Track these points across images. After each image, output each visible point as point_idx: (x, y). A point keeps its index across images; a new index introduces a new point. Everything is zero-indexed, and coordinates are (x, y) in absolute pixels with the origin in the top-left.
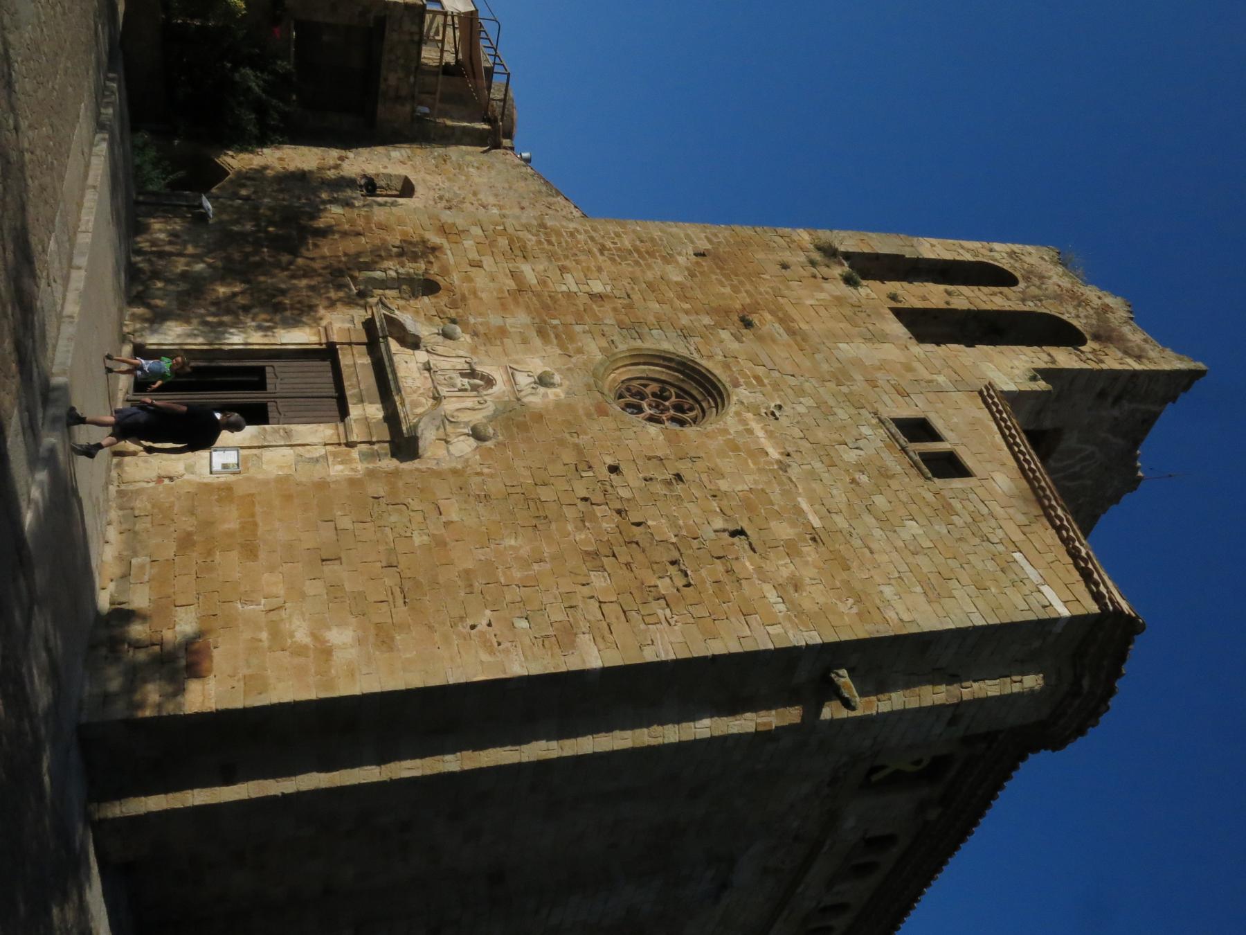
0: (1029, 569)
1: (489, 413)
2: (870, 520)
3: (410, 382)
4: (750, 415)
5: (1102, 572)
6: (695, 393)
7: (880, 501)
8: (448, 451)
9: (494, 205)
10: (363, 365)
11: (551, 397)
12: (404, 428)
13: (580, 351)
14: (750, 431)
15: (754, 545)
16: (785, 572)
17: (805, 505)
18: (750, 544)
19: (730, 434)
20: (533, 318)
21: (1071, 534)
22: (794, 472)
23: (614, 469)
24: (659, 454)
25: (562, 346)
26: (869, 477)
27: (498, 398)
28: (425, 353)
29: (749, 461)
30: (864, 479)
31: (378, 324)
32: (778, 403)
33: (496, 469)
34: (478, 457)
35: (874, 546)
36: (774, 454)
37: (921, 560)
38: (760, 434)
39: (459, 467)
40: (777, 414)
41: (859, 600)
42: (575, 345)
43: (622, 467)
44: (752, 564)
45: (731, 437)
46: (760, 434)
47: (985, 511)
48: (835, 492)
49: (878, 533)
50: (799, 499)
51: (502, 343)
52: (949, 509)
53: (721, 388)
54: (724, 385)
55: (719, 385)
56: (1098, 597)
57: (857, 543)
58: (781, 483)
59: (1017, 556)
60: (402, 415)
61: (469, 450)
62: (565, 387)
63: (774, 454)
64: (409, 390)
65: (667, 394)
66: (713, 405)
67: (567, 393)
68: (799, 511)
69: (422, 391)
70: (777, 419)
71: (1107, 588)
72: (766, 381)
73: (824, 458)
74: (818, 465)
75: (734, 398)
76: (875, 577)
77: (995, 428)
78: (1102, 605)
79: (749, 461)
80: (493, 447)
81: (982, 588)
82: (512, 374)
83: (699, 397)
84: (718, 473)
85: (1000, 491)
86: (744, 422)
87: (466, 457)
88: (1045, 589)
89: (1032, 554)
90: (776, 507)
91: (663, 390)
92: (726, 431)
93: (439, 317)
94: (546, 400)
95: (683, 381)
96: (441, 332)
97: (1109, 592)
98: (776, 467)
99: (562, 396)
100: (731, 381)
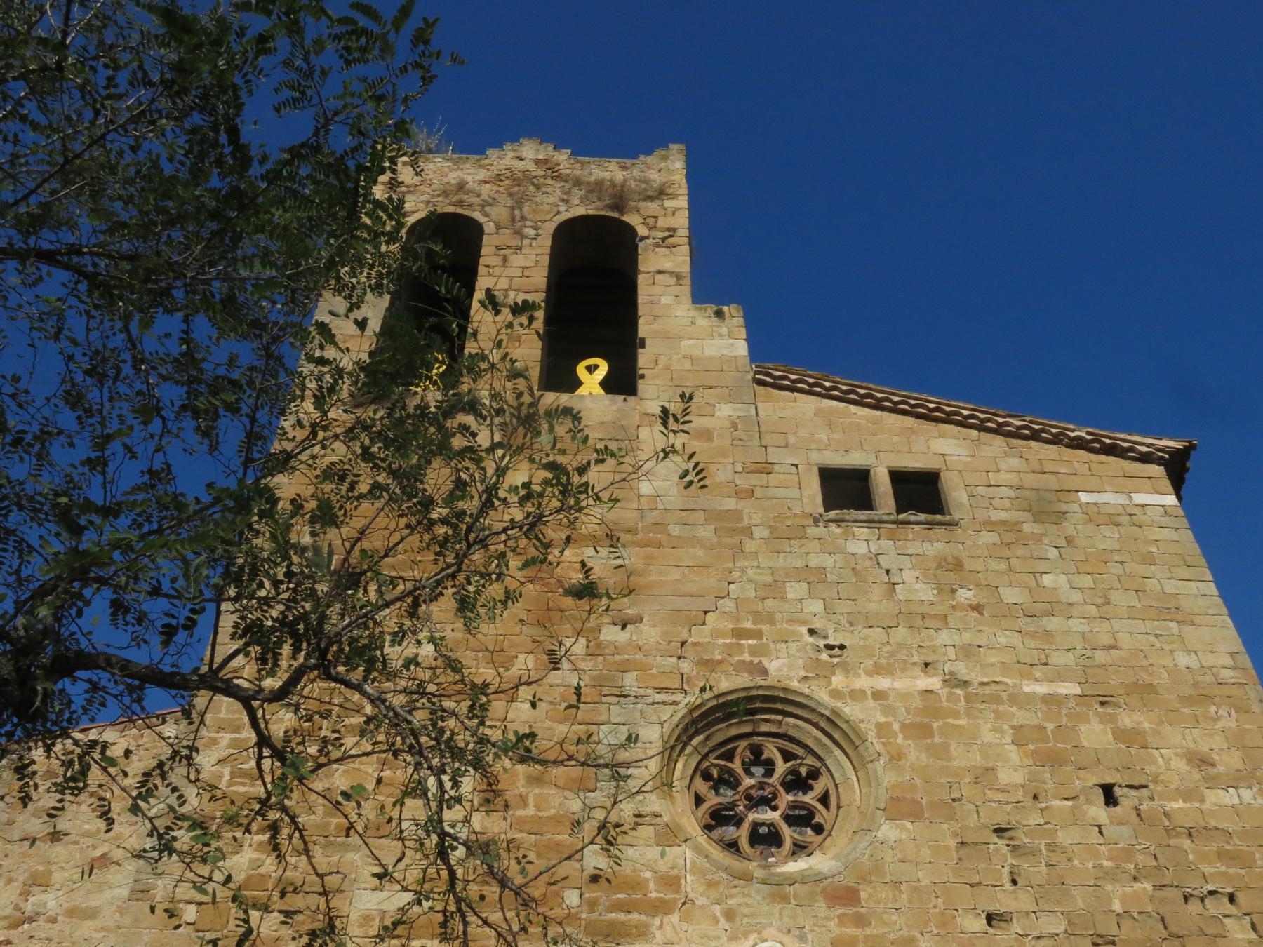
0: (1107, 497)
2: (1053, 623)
4: (838, 680)
5: (1122, 436)
6: (734, 732)
7: (1010, 595)
9: (25, 894)
13: (671, 882)
14: (878, 695)
15: (1136, 783)
16: (1181, 765)
17: (1041, 689)
18: (1131, 787)
19: (889, 724)
21: (1054, 431)
22: (962, 670)
23: (990, 918)
24: (952, 843)
25: (662, 908)
26: (962, 587)
29: (950, 721)
30: (964, 595)
32: (804, 630)
35: (1106, 640)
36: (934, 682)
37: (1115, 597)
38: (883, 683)
40: (831, 642)
41: (1208, 698)
42: (652, 885)
43: (991, 908)
44: (1176, 800)
45: (896, 726)
46: (883, 683)
47: (1012, 493)
48: (1003, 640)
49: (1075, 624)
50: (1026, 689)
52: (1009, 527)
53: (761, 692)
54: (761, 687)
55: (754, 693)
56: (1145, 459)
57: (1100, 657)
58: (996, 699)
59: (1084, 497)
63: (934, 682)
65: (715, 773)
66: (779, 717)
68: (1049, 699)
70: (842, 647)
71: (1143, 444)
72: (748, 625)
73: (928, 622)
74: (944, 637)
75: (795, 684)
76: (1163, 662)
77: (835, 403)
78: (1160, 461)
79: (950, 721)
81: (1150, 560)
83: (747, 729)
84: (983, 777)
85: (969, 459)
86: (857, 695)
88: (1139, 498)
89: (1094, 483)
90: (1050, 726)
91: (707, 776)
92: (882, 729)
95: (707, 739)
97: (1149, 446)
98: (959, 692)
100: (750, 673)
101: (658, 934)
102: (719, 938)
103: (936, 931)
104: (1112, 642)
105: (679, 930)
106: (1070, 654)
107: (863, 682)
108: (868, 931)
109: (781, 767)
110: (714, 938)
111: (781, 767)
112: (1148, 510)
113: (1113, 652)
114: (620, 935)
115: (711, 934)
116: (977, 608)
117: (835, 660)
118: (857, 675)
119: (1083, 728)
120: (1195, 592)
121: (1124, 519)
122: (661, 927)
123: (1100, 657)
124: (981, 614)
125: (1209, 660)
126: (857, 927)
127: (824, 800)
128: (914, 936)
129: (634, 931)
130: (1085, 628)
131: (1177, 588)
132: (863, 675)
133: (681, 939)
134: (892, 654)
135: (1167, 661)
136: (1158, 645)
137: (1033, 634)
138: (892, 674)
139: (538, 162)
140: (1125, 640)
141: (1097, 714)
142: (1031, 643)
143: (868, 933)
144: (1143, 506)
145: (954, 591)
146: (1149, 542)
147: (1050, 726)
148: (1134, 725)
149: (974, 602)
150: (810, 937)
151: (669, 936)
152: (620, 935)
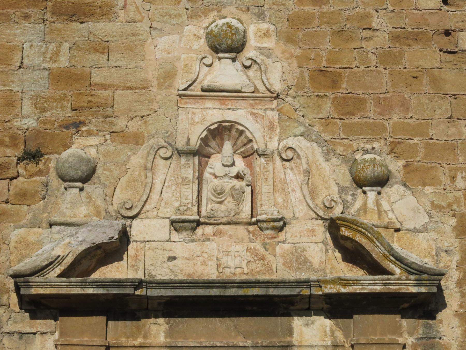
1: (318, 151)
3: (231, 262)
8: (416, 231)
10: (170, 333)
11: (269, 43)
12: (414, 290)
20: (26, 17)
27: (271, 128)
28: (135, 223)
31: (90, 291)
33: (457, 170)
34: (428, 189)
39: (453, 221)
51: (105, 87)
60: (378, 288)
61: (411, 199)
62: (244, 17)
64: (257, 266)
67: (261, 16)
69: (258, 246)
80: (401, 163)
82: (203, 90)
87: (428, 207)
93: (12, 179)
94: (278, 52)
96: (80, 184)
99: (265, 26)
101: (122, 14)
102: (180, 16)
103: (391, 8)
105: (141, 9)
108: (325, 9)
110: (175, 16)
114: (84, 14)
115: (173, 12)
122: (124, 7)
126: (314, 5)
128: (369, 13)
129: (98, 10)
133: (143, 17)
143: (325, 10)
150: (268, 14)
151: (132, 15)
152: (84, 14)
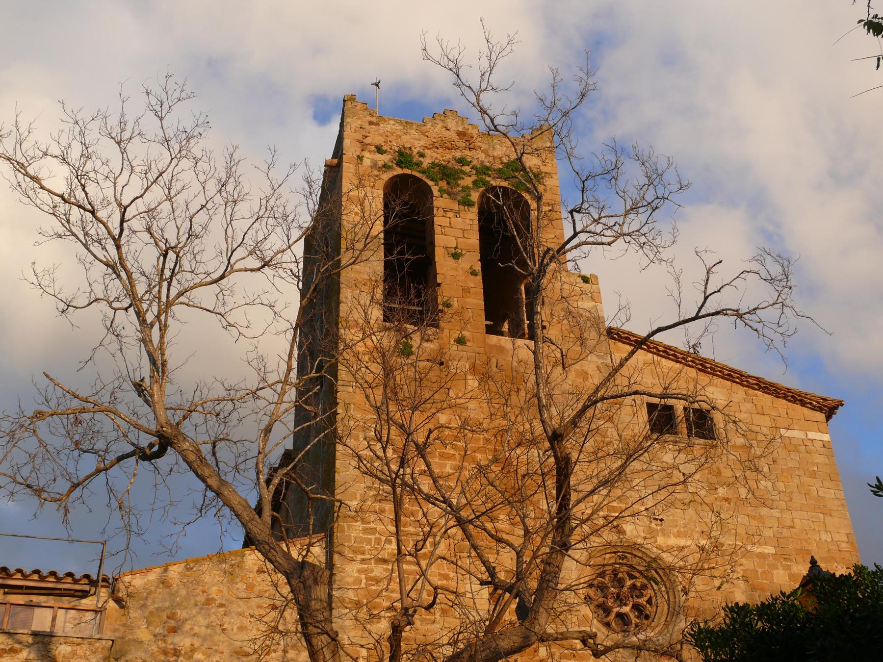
35: (789, 523)
49: (776, 513)
57: (786, 533)
81: (813, 475)
88: (812, 435)
90: (760, 571)
104: (791, 524)
106: (771, 530)
107: (673, 541)
109: (629, 583)
111: (629, 583)
112: (815, 443)
113: (791, 529)
116: (727, 500)
117: (659, 528)
118: (669, 536)
119: (775, 572)
120: (833, 496)
121: (802, 448)
123: (786, 533)
124: (729, 504)
125: (836, 537)
127: (649, 601)
130: (778, 515)
131: (825, 493)
132: (672, 537)
134: (685, 526)
135: (816, 537)
136: (813, 527)
137: (754, 518)
138: (686, 537)
139: (461, 134)
140: (798, 522)
141: (782, 565)
142: (753, 523)
144: (812, 440)
145: (716, 489)
146: (813, 464)
147: (760, 571)
148: (798, 572)
149: (726, 496)
